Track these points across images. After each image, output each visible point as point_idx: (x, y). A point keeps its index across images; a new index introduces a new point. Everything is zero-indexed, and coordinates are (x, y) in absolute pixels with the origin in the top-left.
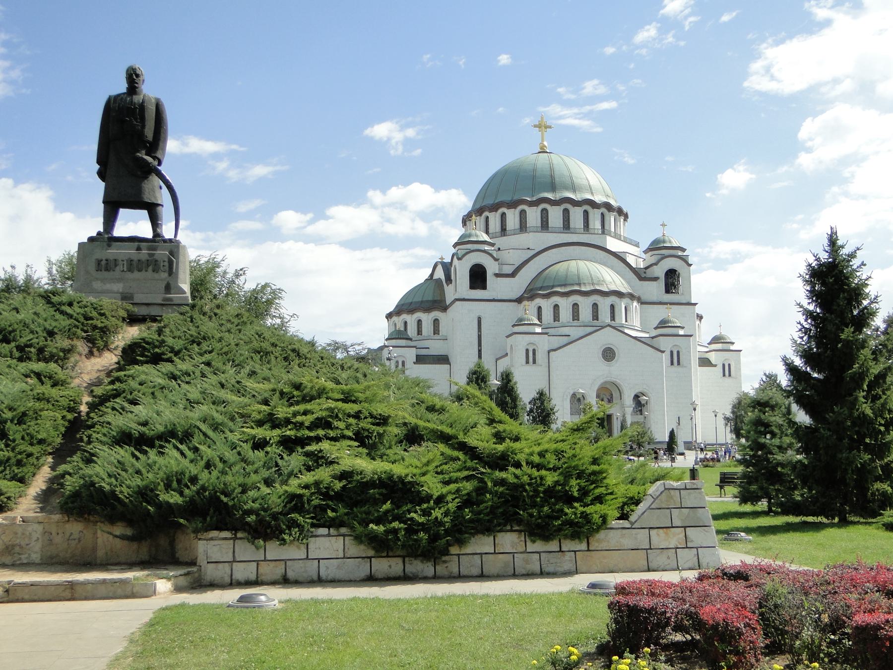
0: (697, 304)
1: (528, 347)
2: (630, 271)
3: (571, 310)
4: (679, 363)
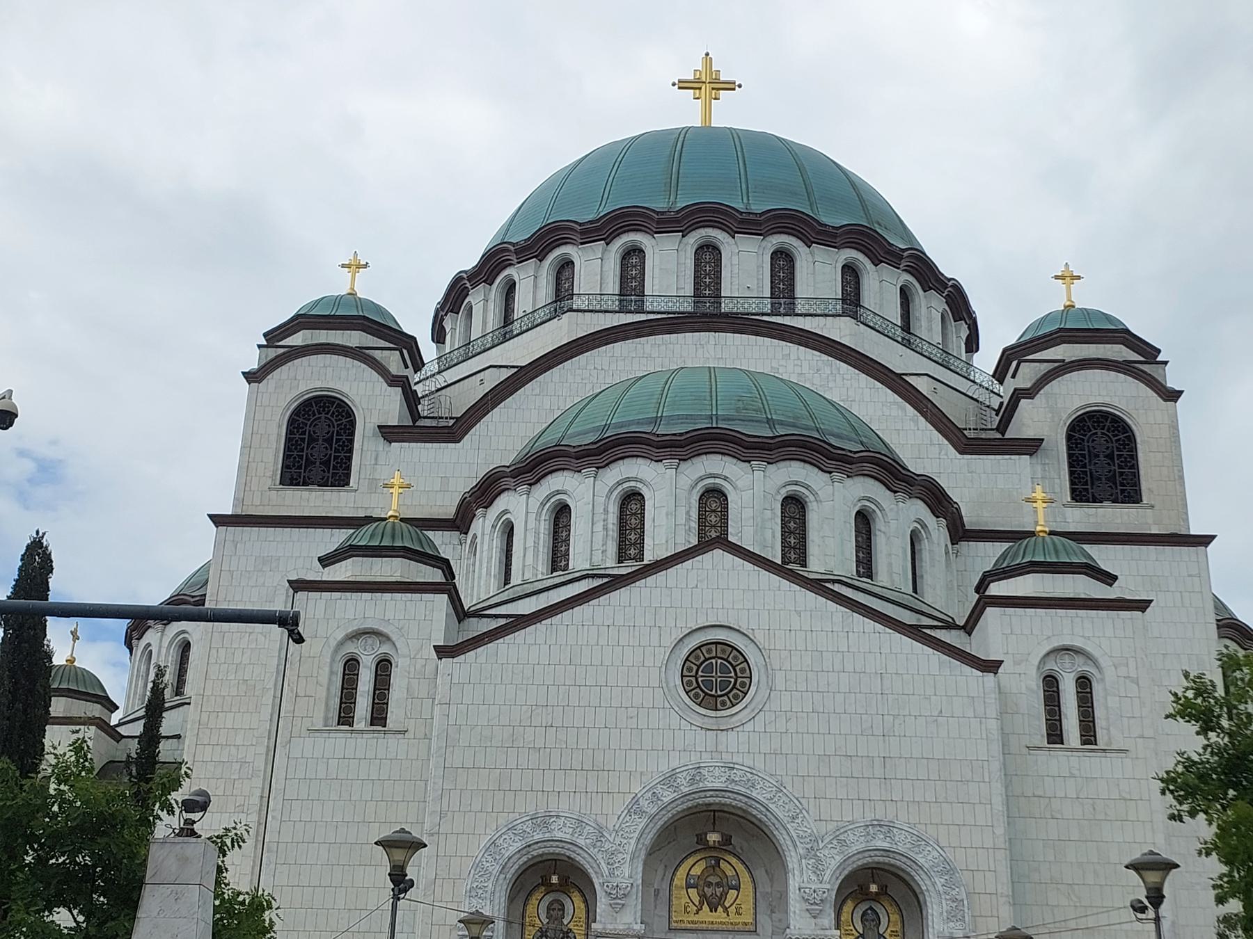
0: (1214, 537)
1: (352, 648)
2: (922, 419)
3: (613, 518)
4: (1088, 734)
